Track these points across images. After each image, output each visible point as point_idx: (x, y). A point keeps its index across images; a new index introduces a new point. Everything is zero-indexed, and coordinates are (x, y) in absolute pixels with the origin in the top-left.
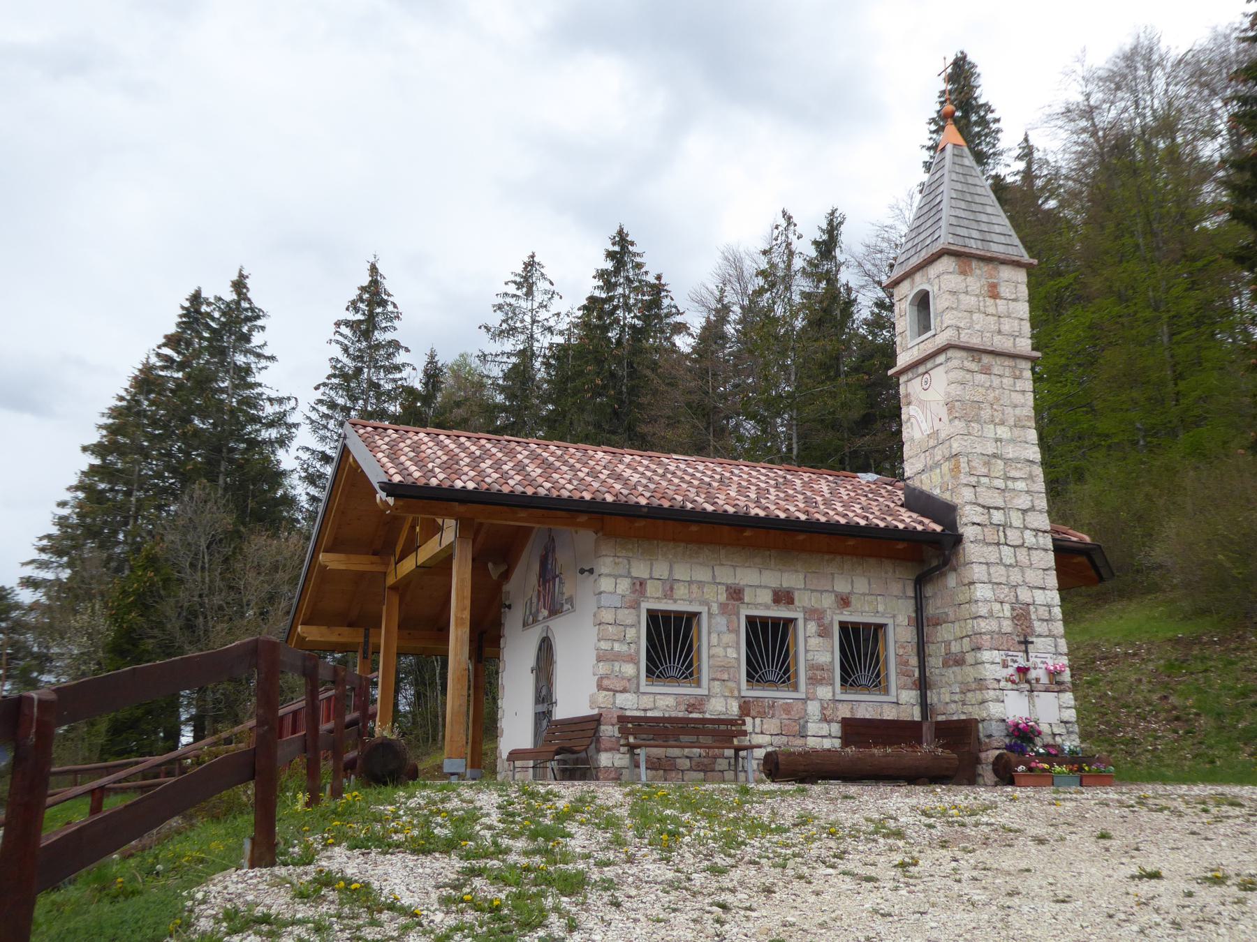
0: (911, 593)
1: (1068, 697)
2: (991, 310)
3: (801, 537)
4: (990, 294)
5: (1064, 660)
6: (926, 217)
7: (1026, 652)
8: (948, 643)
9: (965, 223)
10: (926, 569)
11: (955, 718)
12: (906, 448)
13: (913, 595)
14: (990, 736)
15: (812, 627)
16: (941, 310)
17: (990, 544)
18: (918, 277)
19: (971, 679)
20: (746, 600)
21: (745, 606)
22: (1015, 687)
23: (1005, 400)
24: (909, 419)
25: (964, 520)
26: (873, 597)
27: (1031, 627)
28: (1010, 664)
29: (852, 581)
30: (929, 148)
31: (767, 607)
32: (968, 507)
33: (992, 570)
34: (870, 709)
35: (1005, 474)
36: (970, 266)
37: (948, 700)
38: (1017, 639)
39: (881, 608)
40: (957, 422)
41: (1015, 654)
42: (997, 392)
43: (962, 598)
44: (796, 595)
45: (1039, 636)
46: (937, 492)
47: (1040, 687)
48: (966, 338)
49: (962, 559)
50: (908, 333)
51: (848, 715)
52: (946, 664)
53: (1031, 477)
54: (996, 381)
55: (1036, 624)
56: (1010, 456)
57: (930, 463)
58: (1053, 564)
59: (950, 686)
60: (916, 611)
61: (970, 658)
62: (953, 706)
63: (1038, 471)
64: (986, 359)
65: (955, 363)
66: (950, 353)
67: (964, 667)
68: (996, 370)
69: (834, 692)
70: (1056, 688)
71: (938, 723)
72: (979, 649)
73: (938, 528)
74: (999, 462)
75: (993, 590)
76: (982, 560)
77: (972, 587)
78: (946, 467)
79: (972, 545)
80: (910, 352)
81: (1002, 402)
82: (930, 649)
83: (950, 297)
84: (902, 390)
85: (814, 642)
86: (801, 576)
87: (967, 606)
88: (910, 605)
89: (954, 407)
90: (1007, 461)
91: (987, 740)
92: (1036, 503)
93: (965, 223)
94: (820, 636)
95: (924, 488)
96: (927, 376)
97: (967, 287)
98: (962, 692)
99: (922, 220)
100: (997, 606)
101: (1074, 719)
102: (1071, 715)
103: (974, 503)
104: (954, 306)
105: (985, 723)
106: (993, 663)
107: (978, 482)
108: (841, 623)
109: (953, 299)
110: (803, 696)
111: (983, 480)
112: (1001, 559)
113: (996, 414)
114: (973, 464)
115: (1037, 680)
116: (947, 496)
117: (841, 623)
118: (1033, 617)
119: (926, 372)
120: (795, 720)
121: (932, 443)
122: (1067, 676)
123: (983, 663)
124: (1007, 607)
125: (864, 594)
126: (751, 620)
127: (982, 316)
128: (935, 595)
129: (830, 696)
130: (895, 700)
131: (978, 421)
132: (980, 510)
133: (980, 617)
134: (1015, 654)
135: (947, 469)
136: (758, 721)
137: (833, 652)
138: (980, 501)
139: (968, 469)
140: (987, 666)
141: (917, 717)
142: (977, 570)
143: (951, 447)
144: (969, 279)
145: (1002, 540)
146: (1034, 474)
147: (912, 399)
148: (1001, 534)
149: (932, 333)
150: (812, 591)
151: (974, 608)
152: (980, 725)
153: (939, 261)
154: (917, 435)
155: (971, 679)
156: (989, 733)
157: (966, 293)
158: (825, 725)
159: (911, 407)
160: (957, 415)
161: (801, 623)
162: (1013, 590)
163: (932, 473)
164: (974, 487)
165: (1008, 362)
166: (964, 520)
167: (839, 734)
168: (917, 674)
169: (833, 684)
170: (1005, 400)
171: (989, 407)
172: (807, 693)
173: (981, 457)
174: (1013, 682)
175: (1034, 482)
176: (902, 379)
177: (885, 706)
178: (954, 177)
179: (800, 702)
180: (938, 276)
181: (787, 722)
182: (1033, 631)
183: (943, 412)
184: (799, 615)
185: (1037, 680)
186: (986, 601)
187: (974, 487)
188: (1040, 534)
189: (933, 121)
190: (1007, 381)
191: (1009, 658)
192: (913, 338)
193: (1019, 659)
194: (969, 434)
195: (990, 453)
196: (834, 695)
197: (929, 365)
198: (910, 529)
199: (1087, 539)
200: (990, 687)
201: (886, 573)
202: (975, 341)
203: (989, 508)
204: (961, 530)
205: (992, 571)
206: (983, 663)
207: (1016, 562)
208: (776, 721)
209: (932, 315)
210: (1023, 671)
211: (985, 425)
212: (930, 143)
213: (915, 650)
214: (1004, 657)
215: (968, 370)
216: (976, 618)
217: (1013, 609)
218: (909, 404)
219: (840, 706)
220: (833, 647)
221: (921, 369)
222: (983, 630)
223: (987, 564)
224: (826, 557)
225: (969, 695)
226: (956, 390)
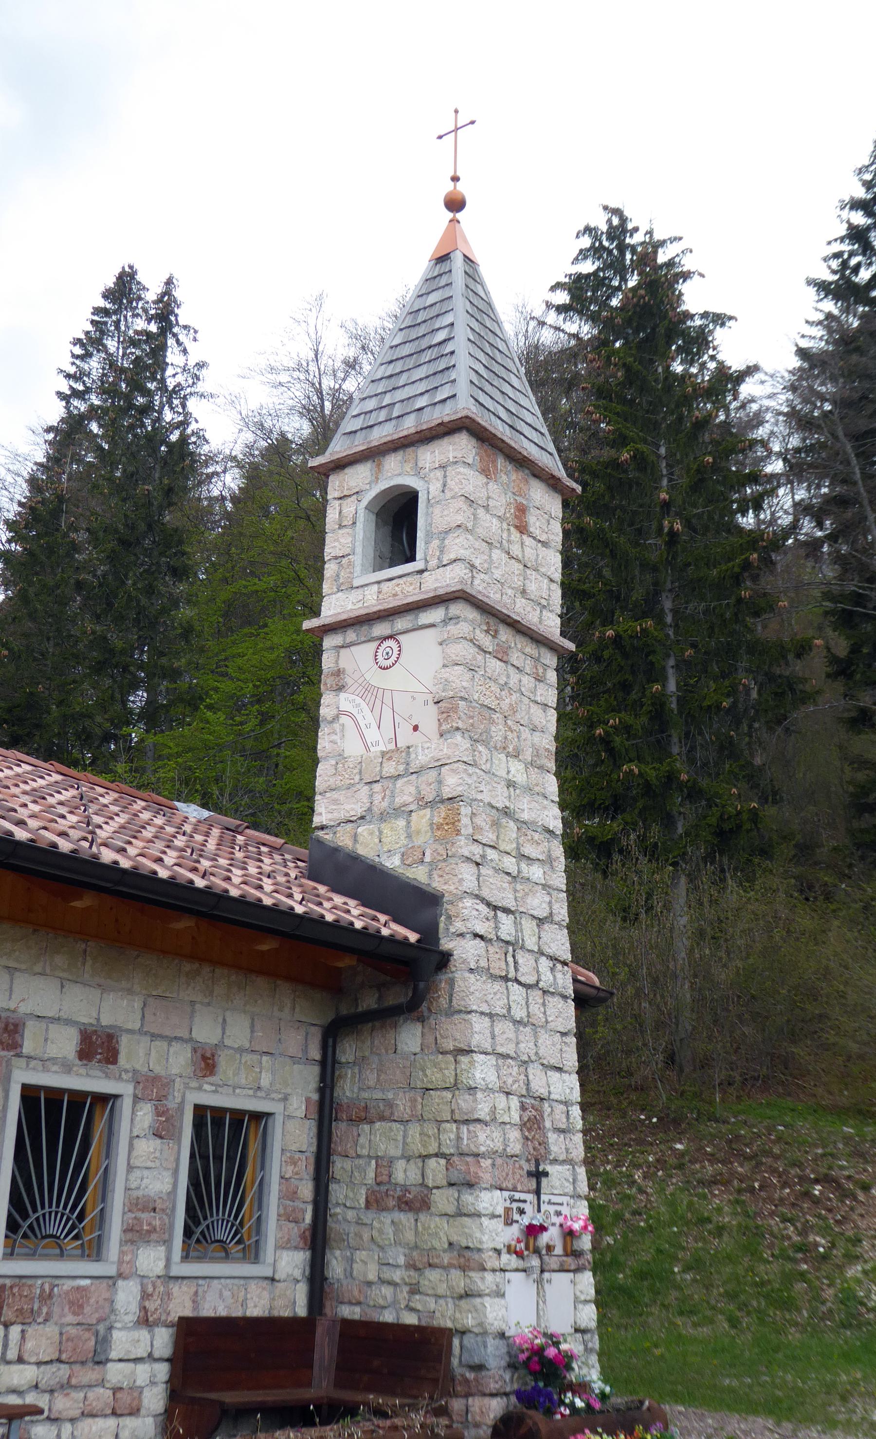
0: (315, 1053)
1: (587, 1281)
2: (516, 550)
3: (184, 924)
4: (516, 522)
5: (583, 1209)
6: (411, 363)
7: (538, 1192)
8: (385, 1164)
9: (488, 388)
10: (344, 1011)
11: (388, 1317)
12: (322, 770)
13: (318, 1056)
14: (479, 1368)
15: (146, 1115)
16: (443, 527)
17: (494, 977)
18: (392, 462)
19: (441, 1244)
20: (28, 1047)
21: (22, 1062)
22: (521, 1264)
23: (521, 716)
24: (336, 718)
25: (458, 926)
26: (256, 1057)
27: (544, 1143)
28: (516, 1217)
29: (224, 1020)
30: (68, 376)
31: (67, 1068)
32: (468, 902)
33: (499, 1027)
34: (227, 1294)
35: (518, 849)
36: (494, 462)
37: (372, 1276)
38: (526, 1167)
39: (265, 1080)
40: (458, 737)
41: (523, 1196)
42: (514, 697)
43: (434, 1076)
44: (124, 1044)
45: (555, 1161)
46: (393, 863)
47: (553, 1262)
48: (479, 587)
49: (444, 1002)
50: (357, 559)
51: (188, 1313)
52: (375, 1202)
53: (549, 861)
54: (515, 676)
55: (552, 1137)
56: (525, 816)
57: (381, 804)
58: (572, 1024)
59: (382, 1248)
60: (321, 1091)
61: (443, 1200)
62: (387, 1291)
63: (558, 851)
64: (505, 635)
65: (463, 628)
66: (458, 609)
67: (422, 1217)
68: (515, 657)
69: (168, 1260)
70: (571, 1262)
71: (347, 1324)
72: (470, 1185)
73: (413, 937)
74: (512, 824)
75: (498, 1068)
76: (485, 1008)
77: (464, 1059)
78: (422, 819)
79: (472, 978)
80: (355, 595)
81: (518, 716)
82: (339, 1166)
83: (465, 507)
84: (327, 661)
85: (147, 1147)
86: (138, 1004)
87: (448, 1095)
88: (311, 1075)
89: (455, 709)
90: (522, 824)
91: (470, 1376)
92: (556, 906)
93: (488, 388)
94: (158, 1135)
95: (361, 851)
96: (391, 643)
97: (488, 498)
98: (412, 1266)
99: (398, 367)
100: (501, 1101)
101: (593, 1325)
102: (589, 1315)
103: (477, 897)
104: (470, 525)
105: (468, 1340)
106: (493, 1216)
107: (483, 856)
108: (200, 1111)
109: (469, 512)
110: (112, 1271)
111: (491, 854)
112: (509, 1009)
113: (510, 735)
114: (478, 821)
115: (549, 1248)
116: (419, 875)
117: (200, 1111)
118: (548, 1124)
119: (391, 637)
120: (89, 1327)
121: (390, 768)
122: (586, 1243)
123: (479, 1215)
124: (515, 1102)
125: (241, 1050)
126: (30, 1095)
127: (504, 556)
128: (361, 1062)
129: (159, 1268)
130: (269, 1274)
131: (486, 743)
132: (482, 908)
133: (478, 1120)
134: (523, 1196)
135: (425, 821)
136: (15, 1331)
137: (176, 1172)
138: (485, 893)
139: (471, 831)
140: (485, 1221)
141: (302, 1311)
142: (477, 1027)
143: (440, 782)
144: (492, 486)
145: (512, 975)
146: (554, 856)
147: (349, 681)
148: (510, 959)
149: (417, 565)
150: (154, 1036)
151: (464, 1102)
152: (456, 1342)
153: (446, 440)
154: (353, 748)
155: (441, 1244)
156: (477, 1361)
157: (486, 508)
158: (144, 1334)
159: (343, 695)
160: (460, 725)
161: (126, 1104)
162: (522, 1069)
163: (386, 828)
164: (478, 864)
165: (531, 649)
166: (458, 926)
167: (167, 1352)
168: (308, 1217)
169: (168, 1243)
170: (521, 716)
171: (501, 721)
172: (120, 1262)
173: (488, 809)
174: (519, 1254)
175: (552, 867)
176: (329, 642)
177: (253, 1286)
178: (469, 307)
179: (104, 1283)
180: (443, 467)
181: (73, 1331)
182: (548, 1151)
183: (429, 718)
184: (124, 1089)
185: (549, 1248)
186: (488, 1089)
187: (478, 864)
188: (559, 966)
189: (77, 342)
190: (528, 682)
191: (515, 1205)
192: (364, 571)
193: (528, 1208)
194: (474, 765)
195: (500, 805)
196: (168, 1266)
197: (401, 623)
198: (371, 931)
199: (596, 981)
200: (489, 1265)
201: (281, 1010)
202: (494, 597)
203: (495, 908)
204: (446, 944)
205: (497, 1031)
206: (479, 1215)
207: (528, 1016)
208: (51, 1330)
209: (420, 534)
210: (533, 1231)
211: (495, 753)
212: (72, 370)
213: (311, 1168)
214: (508, 1204)
215: (479, 647)
216: (467, 1122)
217: (523, 1108)
218: (340, 688)
219: (176, 1289)
220: (177, 1160)
221: (381, 629)
222: (483, 1149)
223: (491, 1016)
224: (187, 967)
225: (433, 1275)
226: (459, 678)
